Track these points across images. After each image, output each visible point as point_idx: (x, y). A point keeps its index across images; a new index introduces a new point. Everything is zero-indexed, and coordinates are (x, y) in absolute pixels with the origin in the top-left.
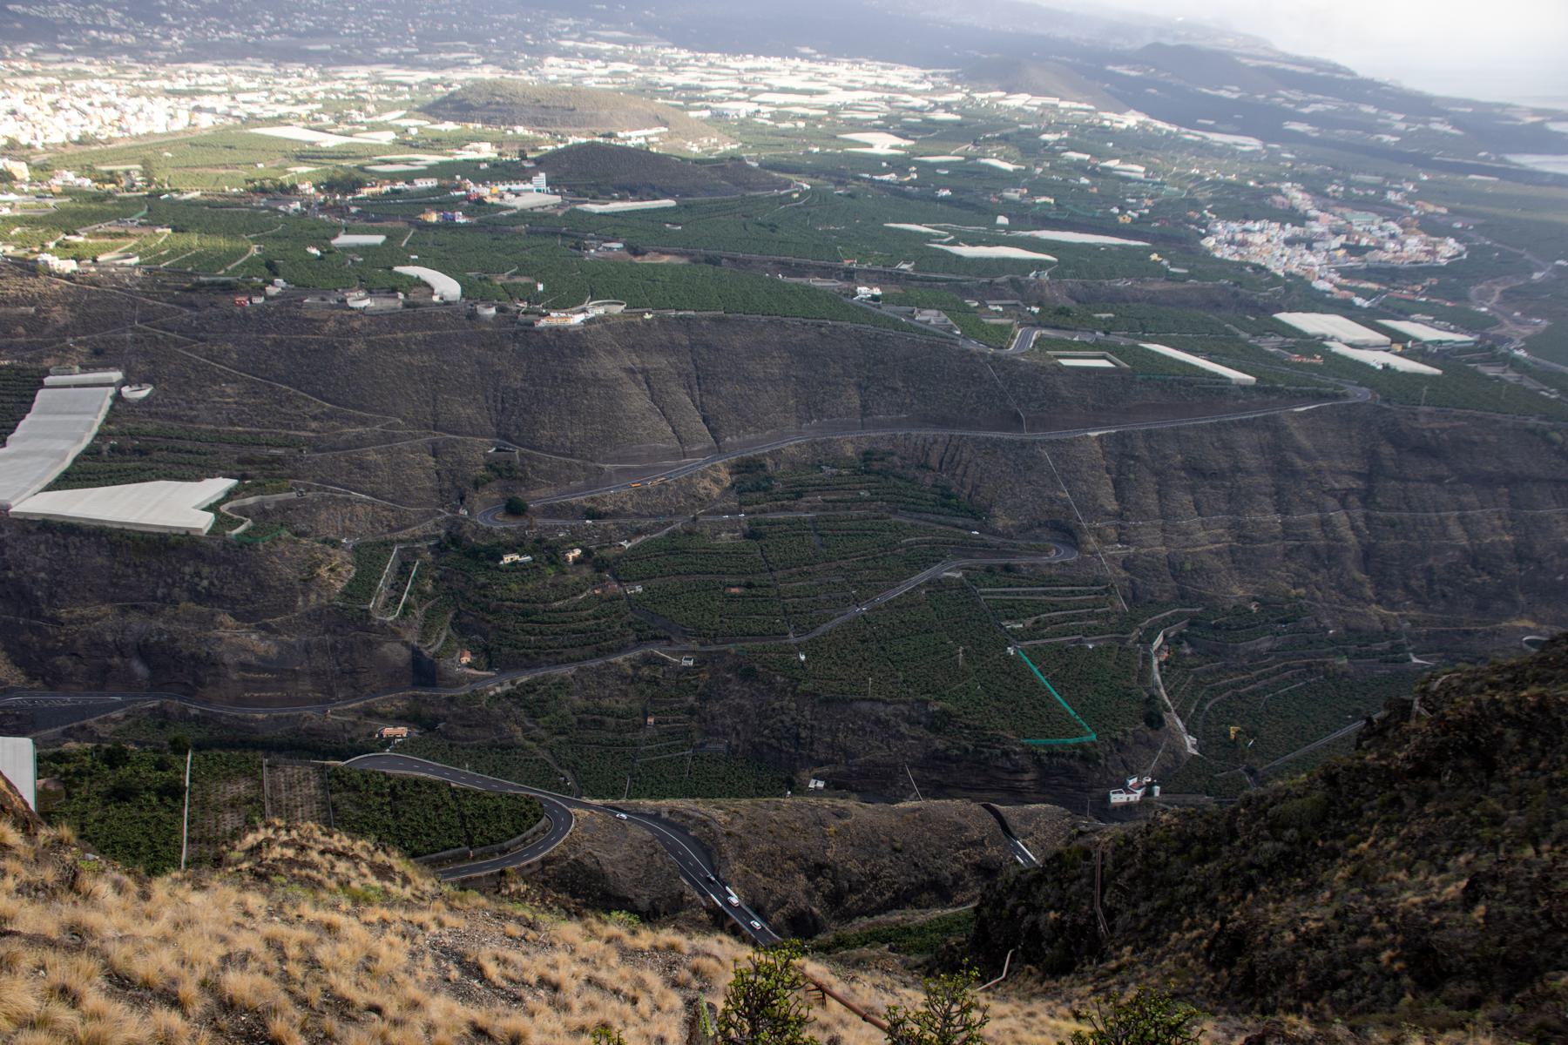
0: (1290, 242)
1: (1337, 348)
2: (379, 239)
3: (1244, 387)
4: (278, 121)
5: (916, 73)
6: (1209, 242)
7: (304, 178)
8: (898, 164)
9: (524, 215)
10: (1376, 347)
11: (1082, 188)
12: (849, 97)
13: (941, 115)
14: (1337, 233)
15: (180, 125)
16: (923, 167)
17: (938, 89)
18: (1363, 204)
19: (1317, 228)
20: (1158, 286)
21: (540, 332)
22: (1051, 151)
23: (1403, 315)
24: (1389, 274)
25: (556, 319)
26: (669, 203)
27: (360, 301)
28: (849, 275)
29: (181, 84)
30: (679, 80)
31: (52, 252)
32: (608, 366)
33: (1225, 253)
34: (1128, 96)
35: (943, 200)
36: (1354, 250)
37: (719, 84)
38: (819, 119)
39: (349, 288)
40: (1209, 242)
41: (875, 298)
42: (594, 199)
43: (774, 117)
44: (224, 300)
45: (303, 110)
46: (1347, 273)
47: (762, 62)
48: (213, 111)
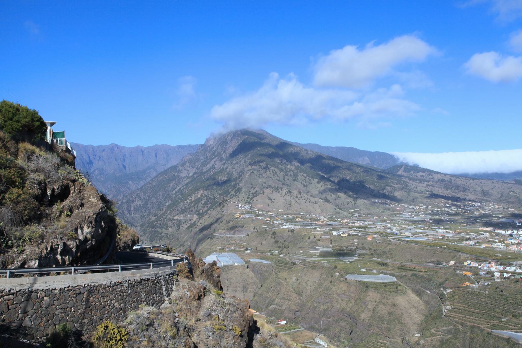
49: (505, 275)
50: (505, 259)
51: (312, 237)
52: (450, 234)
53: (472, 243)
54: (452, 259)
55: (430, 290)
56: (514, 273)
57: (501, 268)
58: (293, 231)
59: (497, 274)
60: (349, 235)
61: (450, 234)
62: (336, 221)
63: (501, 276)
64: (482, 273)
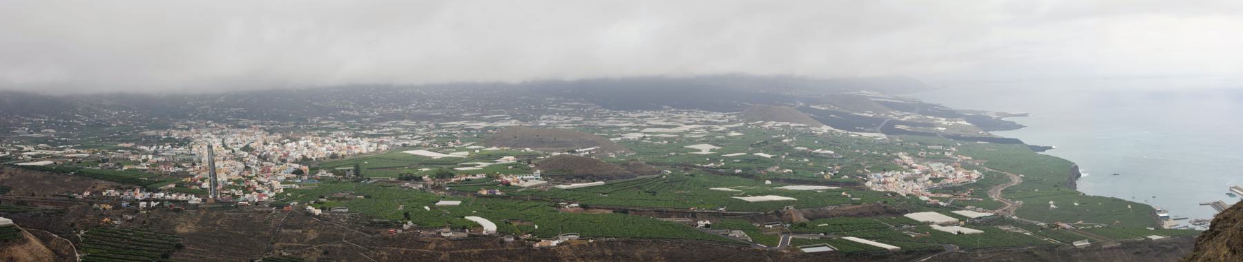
0: (905, 180)
1: (936, 227)
2: (458, 203)
3: (894, 252)
4: (414, 148)
5: (720, 115)
7: (425, 173)
8: (714, 158)
9: (529, 190)
10: (953, 224)
11: (805, 164)
12: (687, 128)
14: (927, 173)
15: (371, 150)
17: (731, 122)
18: (936, 159)
19: (917, 171)
20: (849, 207)
21: (535, 250)
22: (788, 148)
23: (962, 207)
24: (953, 189)
27: (447, 233)
28: (694, 215)
29: (375, 132)
30: (604, 124)
34: (824, 119)
36: (935, 180)
37: (624, 125)
38: (674, 139)
41: (707, 226)
42: (564, 183)
43: (652, 139)
44: (384, 232)
45: (427, 143)
46: (934, 191)
47: (646, 113)
48: (388, 143)
49: (153, 204)
50: (149, 183)
53: (111, 165)
56: (162, 201)
57: (147, 195)
59: (143, 204)
63: (148, 208)
64: (124, 204)
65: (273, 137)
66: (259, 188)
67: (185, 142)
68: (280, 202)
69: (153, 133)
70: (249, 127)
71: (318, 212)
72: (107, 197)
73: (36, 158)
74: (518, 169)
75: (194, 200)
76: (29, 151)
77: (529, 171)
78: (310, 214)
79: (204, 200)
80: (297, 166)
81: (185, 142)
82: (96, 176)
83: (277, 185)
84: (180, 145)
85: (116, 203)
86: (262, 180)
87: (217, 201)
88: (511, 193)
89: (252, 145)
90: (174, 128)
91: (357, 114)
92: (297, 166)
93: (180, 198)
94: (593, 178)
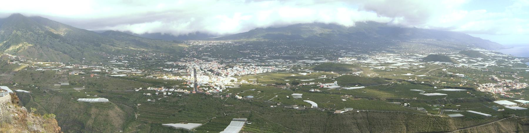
6: (479, 88)
7: (287, 82)
9: (332, 90)
13: (421, 67)
15: (265, 72)
16: (418, 77)
25: (338, 112)
26: (363, 87)
31: (238, 95)
32: (349, 122)
33: (483, 90)
35: (422, 84)
39: (294, 104)
40: (479, 88)
42: (347, 87)
49: (169, 94)
50: (169, 84)
51: (56, 76)
52: (139, 72)
54: (141, 87)
55: (128, 105)
56: (173, 92)
57: (167, 90)
58: (43, 72)
59: (165, 93)
60: (80, 74)
61: (139, 72)
62: (71, 66)
64: (157, 93)
65: (221, 66)
66: (215, 87)
67: (184, 68)
68: (224, 93)
69: (170, 63)
70: (211, 61)
71: (241, 98)
72: (150, 90)
73: (119, 73)
74: (328, 81)
75: (187, 91)
76: (116, 69)
77: (332, 82)
78: (236, 99)
79: (191, 92)
80: (232, 78)
81: (184, 68)
82: (145, 81)
83: (223, 86)
84: (182, 69)
85: (153, 92)
86: (217, 84)
87: (198, 93)
88: (325, 91)
89: (213, 69)
90: (180, 61)
91: (259, 56)
92: (232, 78)
93: (181, 91)
94: (360, 85)
